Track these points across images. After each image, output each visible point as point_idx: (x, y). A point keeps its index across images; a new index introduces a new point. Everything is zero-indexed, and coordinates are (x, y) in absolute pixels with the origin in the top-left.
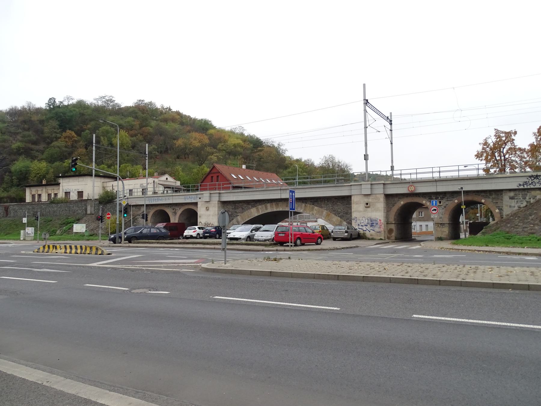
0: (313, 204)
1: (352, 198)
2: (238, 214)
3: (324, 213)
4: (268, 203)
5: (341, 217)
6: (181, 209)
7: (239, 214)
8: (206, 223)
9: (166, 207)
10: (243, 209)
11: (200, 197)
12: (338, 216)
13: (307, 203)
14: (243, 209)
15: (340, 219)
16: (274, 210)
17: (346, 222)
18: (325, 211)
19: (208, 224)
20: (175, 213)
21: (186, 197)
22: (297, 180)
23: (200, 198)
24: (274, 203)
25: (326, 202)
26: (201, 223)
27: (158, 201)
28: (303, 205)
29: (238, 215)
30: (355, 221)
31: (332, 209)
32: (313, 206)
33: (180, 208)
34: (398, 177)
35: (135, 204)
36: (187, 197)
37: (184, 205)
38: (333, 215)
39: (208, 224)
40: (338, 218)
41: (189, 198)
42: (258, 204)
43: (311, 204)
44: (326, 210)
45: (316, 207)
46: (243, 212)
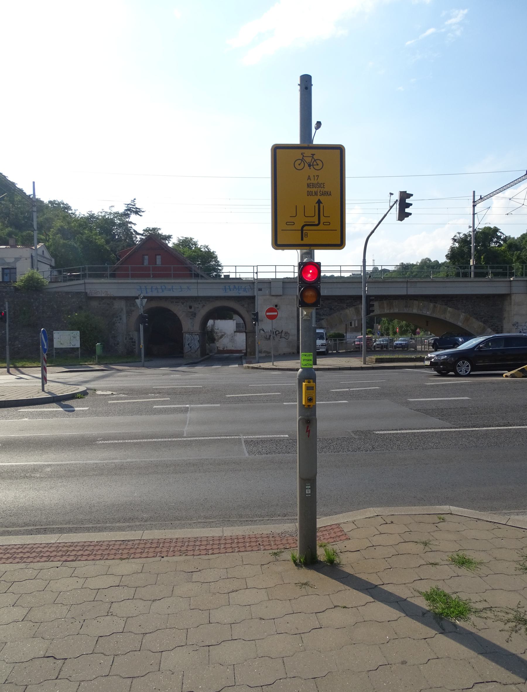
0: (445, 305)
1: (513, 297)
2: (322, 317)
3: (461, 317)
4: (376, 300)
5: (485, 322)
7: (324, 317)
8: (274, 331)
9: (173, 302)
10: (331, 309)
12: (481, 321)
13: (436, 303)
14: (331, 309)
15: (482, 324)
16: (386, 311)
17: (491, 329)
18: (463, 314)
19: (277, 332)
20: (194, 315)
21: (227, 287)
22: (172, 272)
23: (260, 290)
24: (385, 302)
25: (464, 302)
26: (264, 331)
27: (163, 291)
28: (432, 305)
29: (323, 319)
30: (516, 327)
31: (472, 311)
32: (446, 306)
33: (204, 306)
34: (326, 275)
35: (103, 295)
36: (229, 286)
38: (474, 320)
39: (277, 332)
40: (480, 323)
41: (235, 287)
42: (359, 302)
43: (443, 305)
44: (464, 313)
45: (449, 309)
46: (331, 314)
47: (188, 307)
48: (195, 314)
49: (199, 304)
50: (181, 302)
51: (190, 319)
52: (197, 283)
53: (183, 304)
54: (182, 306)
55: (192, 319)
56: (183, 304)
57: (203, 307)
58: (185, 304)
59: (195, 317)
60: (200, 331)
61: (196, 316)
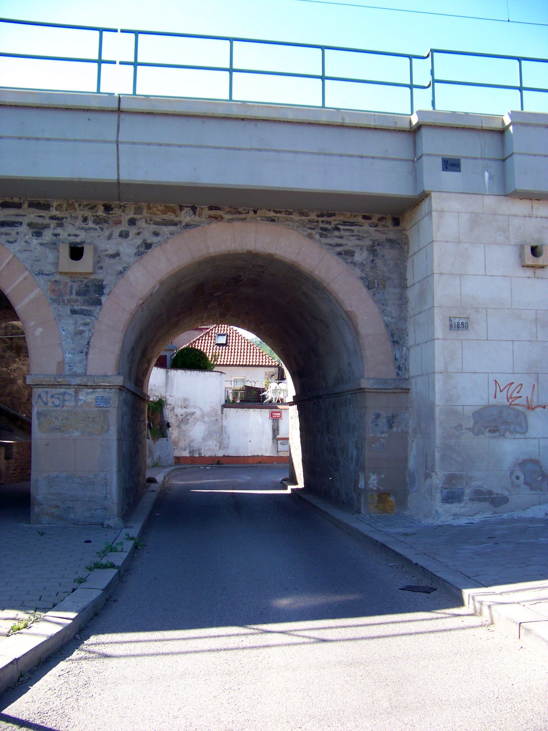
6: (155, 252)
11: (451, 153)
33: (148, 246)
37: (186, 217)
47: (65, 251)
48: (100, 288)
49: (124, 235)
50: (30, 225)
51: (74, 312)
52: (117, 143)
53: (38, 234)
54: (35, 242)
55: (82, 312)
56: (38, 234)
57: (139, 254)
58: (47, 236)
59: (99, 303)
60: (119, 381)
61: (104, 299)
